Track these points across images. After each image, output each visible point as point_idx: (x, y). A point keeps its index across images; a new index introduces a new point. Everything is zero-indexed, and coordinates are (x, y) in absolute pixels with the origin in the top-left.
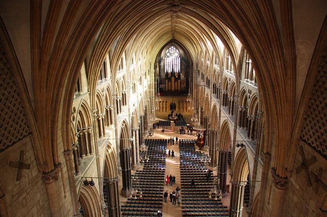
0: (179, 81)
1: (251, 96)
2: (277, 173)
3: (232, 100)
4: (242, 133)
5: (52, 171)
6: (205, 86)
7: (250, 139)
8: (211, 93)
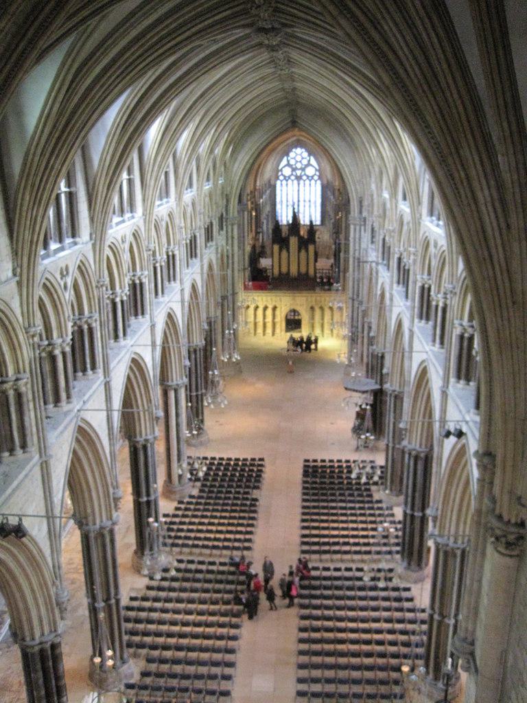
0: (311, 248)
3: (441, 305)
4: (461, 398)
6: (377, 264)
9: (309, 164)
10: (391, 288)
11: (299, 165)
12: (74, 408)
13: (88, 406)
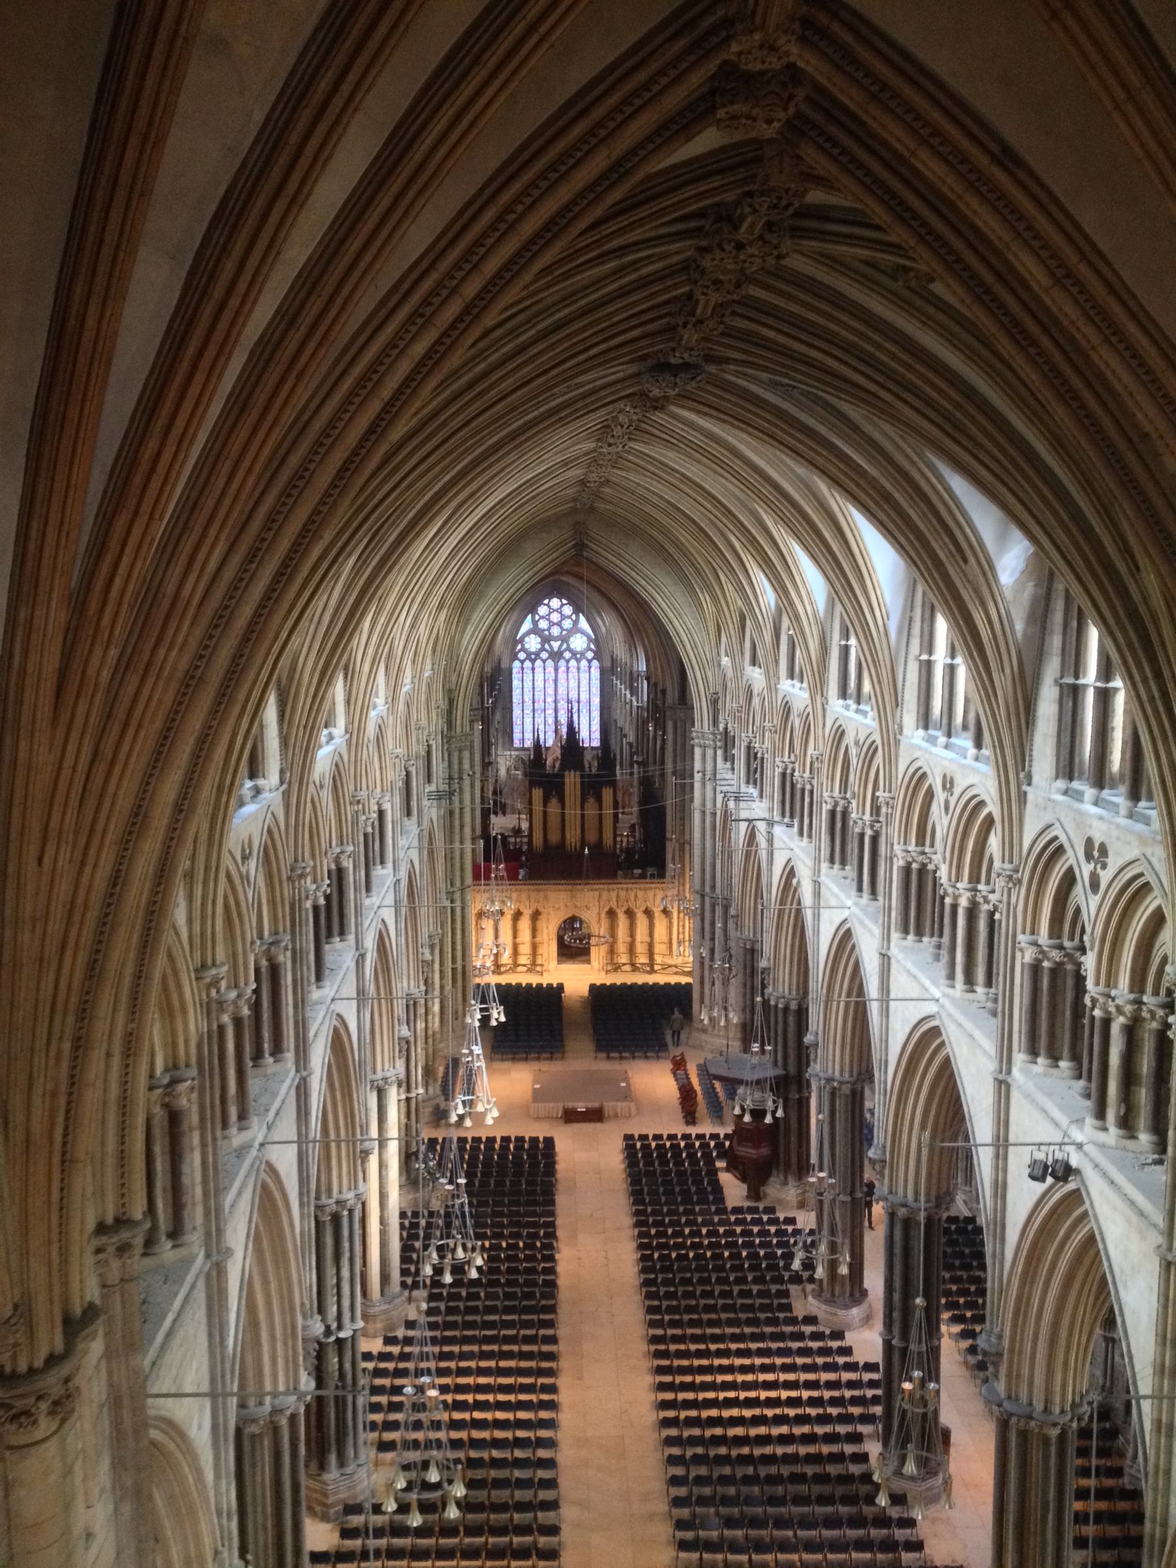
0: (607, 794)
1: (1105, 877)
3: (964, 902)
4: (1049, 1095)
6: (771, 823)
7: (1113, 1134)
8: (817, 860)
9: (575, 629)
10: (817, 871)
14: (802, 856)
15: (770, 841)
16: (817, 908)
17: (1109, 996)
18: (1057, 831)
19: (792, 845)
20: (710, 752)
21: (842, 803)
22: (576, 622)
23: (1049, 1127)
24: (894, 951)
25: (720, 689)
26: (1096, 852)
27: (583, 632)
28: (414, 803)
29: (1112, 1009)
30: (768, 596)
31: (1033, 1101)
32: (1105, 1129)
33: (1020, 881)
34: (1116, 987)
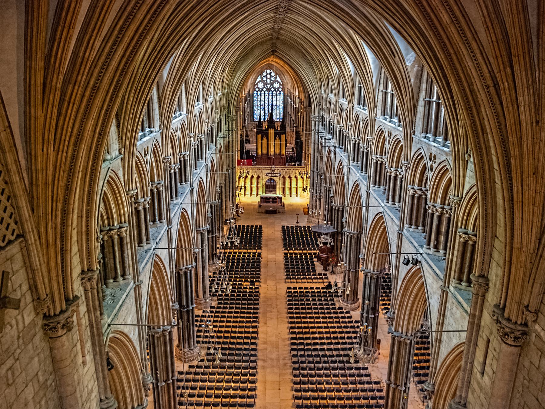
0: (283, 137)
1: (435, 166)
2: (506, 315)
3: (393, 174)
5: (62, 312)
6: (335, 147)
8: (349, 160)
9: (276, 81)
10: (349, 164)
11: (269, 81)
12: (151, 247)
13: (159, 246)
14: (345, 159)
15: (335, 154)
16: (348, 176)
17: (433, 206)
18: (422, 151)
19: (342, 155)
20: (317, 123)
21: (358, 140)
22: (276, 78)
23: (413, 248)
24: (371, 191)
25: (321, 101)
26: (433, 158)
27: (278, 82)
28: (214, 139)
29: (435, 210)
30: (336, 70)
31: (409, 240)
32: (430, 249)
33: (410, 167)
34: (436, 203)
